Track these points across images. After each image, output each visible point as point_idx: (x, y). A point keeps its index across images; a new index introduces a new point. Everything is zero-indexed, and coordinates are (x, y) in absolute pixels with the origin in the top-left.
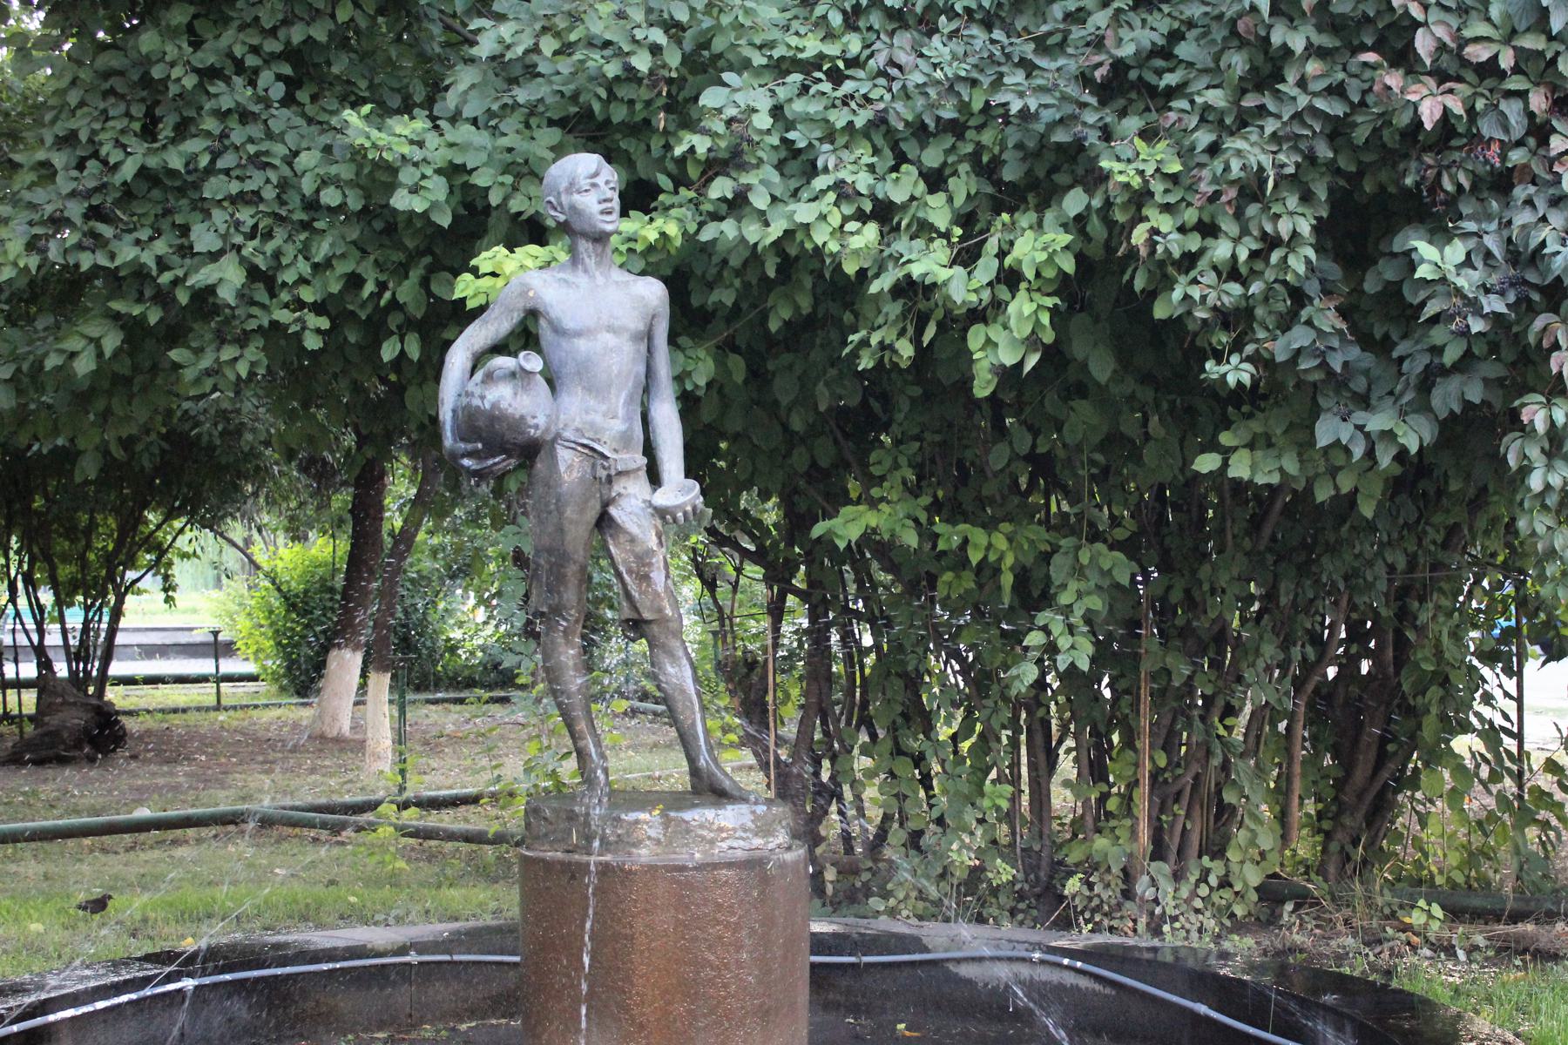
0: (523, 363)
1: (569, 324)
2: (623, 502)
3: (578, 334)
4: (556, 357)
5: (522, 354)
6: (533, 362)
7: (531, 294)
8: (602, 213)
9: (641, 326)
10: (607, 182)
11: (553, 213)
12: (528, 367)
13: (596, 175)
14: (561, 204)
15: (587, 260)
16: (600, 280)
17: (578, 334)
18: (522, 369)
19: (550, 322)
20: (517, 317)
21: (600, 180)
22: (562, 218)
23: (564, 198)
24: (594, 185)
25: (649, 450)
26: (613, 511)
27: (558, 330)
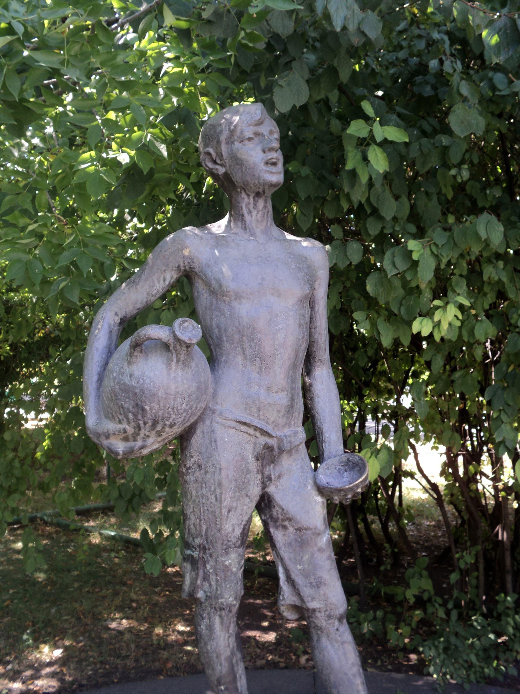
0: (178, 333)
1: (230, 285)
2: (283, 481)
3: (238, 296)
4: (215, 320)
5: (177, 323)
6: (188, 330)
7: (186, 253)
8: (267, 163)
9: (307, 290)
10: (271, 132)
11: (210, 165)
12: (184, 337)
13: (260, 123)
14: (220, 155)
15: (247, 217)
16: (261, 238)
17: (238, 296)
18: (177, 340)
19: (208, 284)
20: (171, 276)
21: (264, 129)
22: (221, 171)
23: (224, 148)
24: (257, 134)
25: (309, 417)
26: (271, 489)
27: (217, 292)
